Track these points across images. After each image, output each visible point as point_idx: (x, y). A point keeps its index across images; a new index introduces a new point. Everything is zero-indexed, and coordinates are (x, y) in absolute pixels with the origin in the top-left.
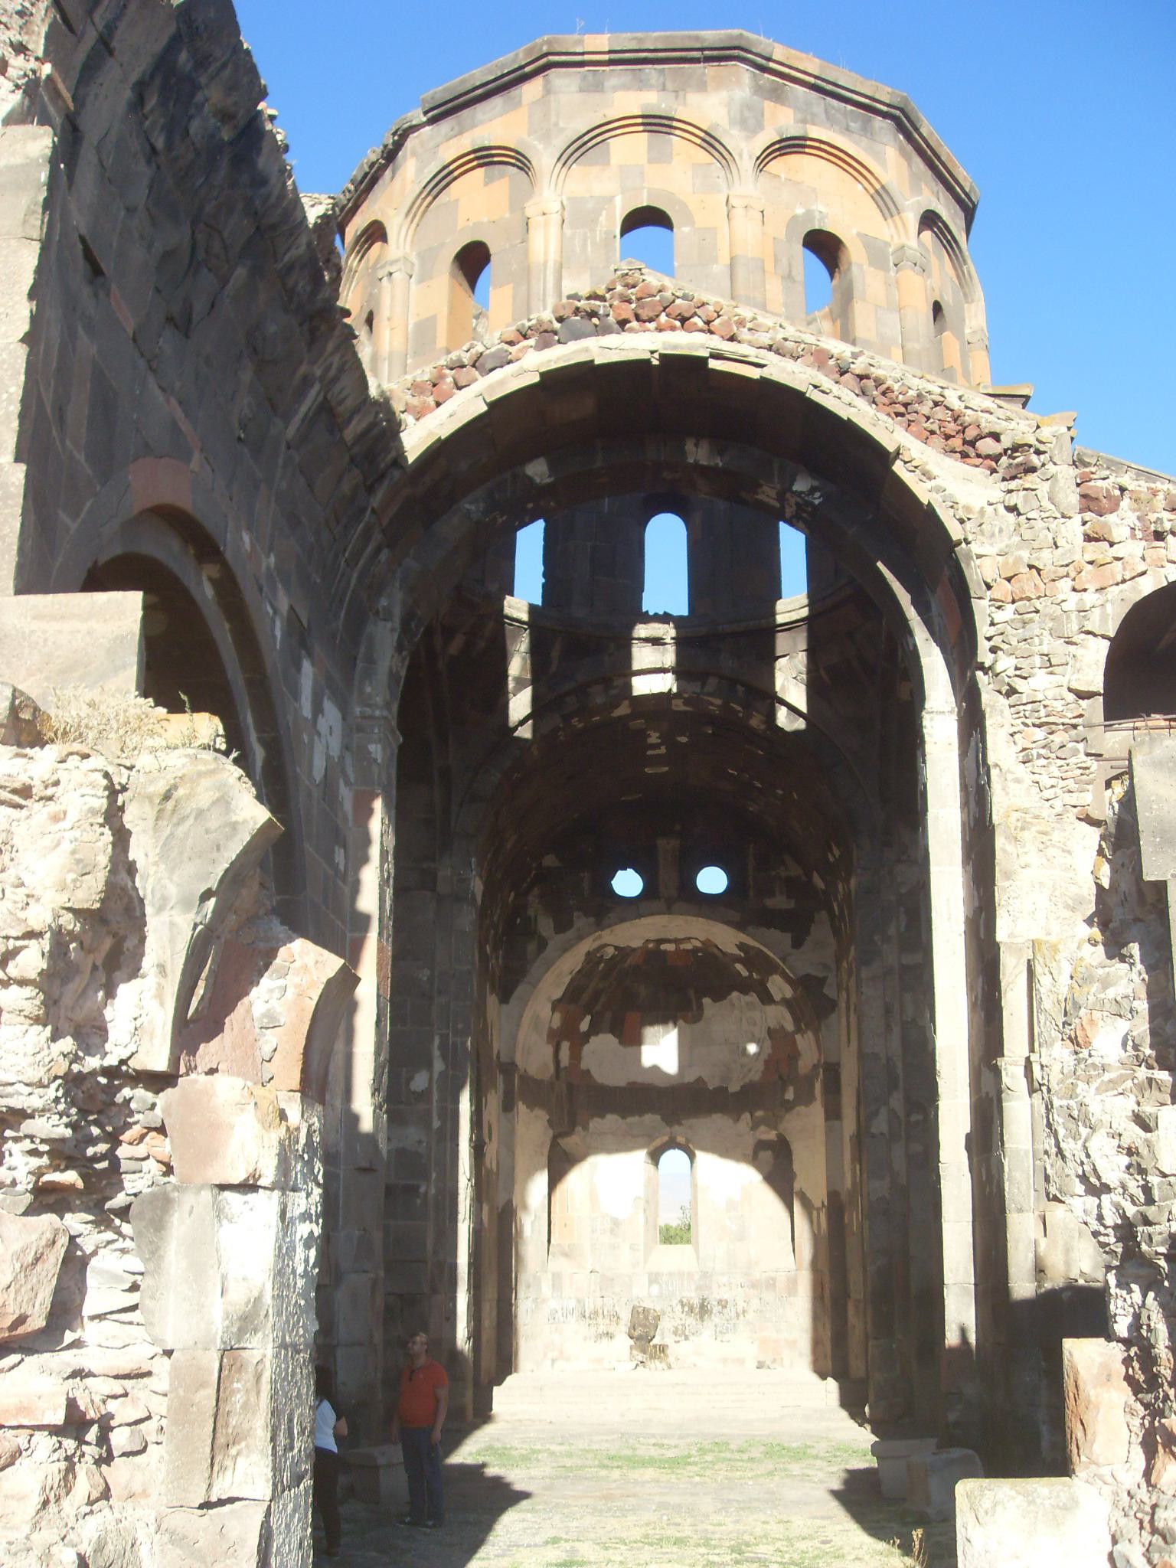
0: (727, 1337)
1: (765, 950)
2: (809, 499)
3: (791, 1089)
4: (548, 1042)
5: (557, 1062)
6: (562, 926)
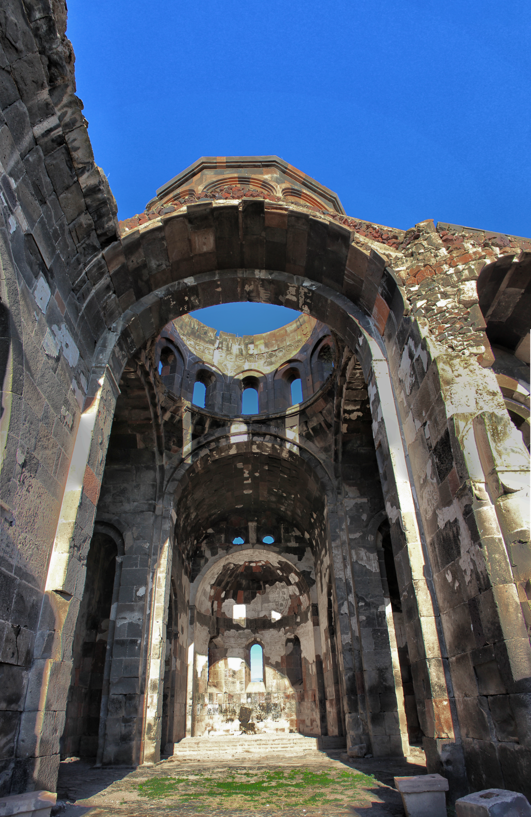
0: (277, 720)
1: (288, 562)
2: (311, 288)
5: (213, 609)
6: (214, 553)
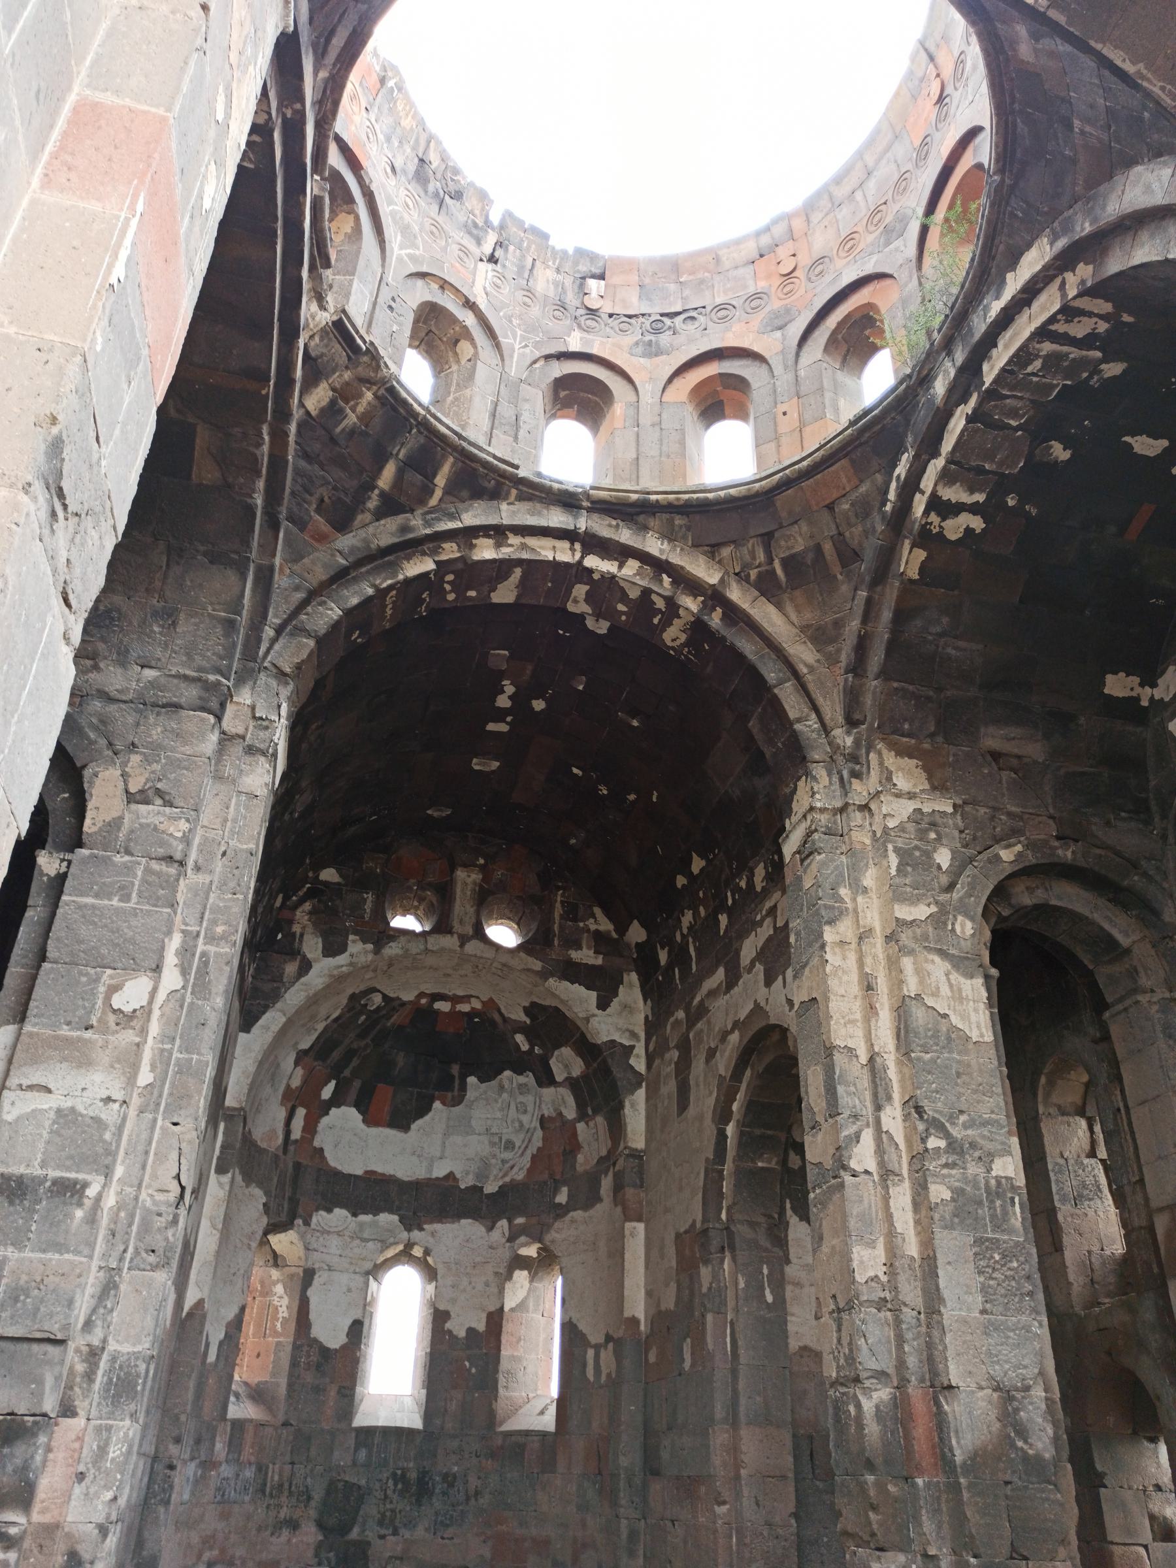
0: (450, 1532)
3: (565, 1190)
4: (282, 1104)
5: (288, 1132)
6: (333, 949)
